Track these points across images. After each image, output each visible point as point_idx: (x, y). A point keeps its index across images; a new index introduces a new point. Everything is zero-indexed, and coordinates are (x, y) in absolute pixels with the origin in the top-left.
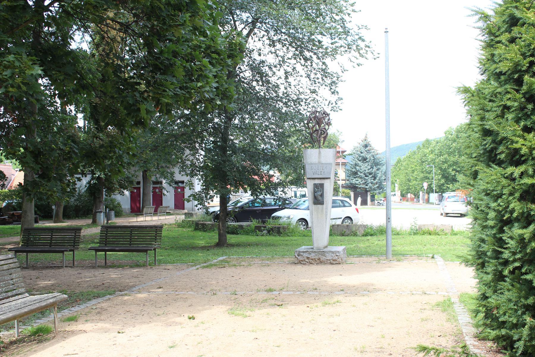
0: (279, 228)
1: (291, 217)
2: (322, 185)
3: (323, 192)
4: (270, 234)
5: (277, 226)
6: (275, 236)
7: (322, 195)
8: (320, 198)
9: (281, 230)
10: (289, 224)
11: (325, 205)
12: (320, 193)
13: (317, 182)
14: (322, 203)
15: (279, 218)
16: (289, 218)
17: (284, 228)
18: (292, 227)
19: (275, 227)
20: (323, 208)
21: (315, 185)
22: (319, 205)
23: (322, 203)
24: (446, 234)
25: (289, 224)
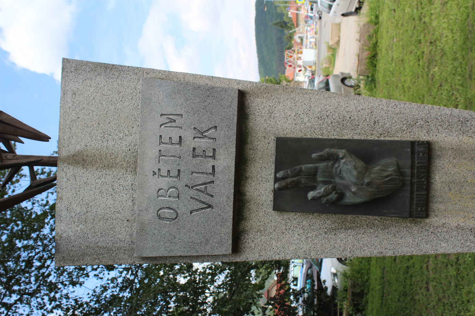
0: (354, 294)
1: (334, 271)
2: (290, 151)
3: (341, 143)
4: (364, 310)
5: (349, 296)
6: (367, 302)
7: (366, 152)
8: (385, 168)
9: (358, 290)
10: (345, 275)
11: (442, 138)
12: (348, 168)
13: (262, 185)
14: (422, 156)
15: (334, 288)
16: (335, 275)
17: (354, 286)
18: (349, 273)
19: (353, 300)
20: (459, 152)
21: (290, 197)
22: (439, 179)
23: (422, 156)
24: (376, 32)
25: (345, 275)
